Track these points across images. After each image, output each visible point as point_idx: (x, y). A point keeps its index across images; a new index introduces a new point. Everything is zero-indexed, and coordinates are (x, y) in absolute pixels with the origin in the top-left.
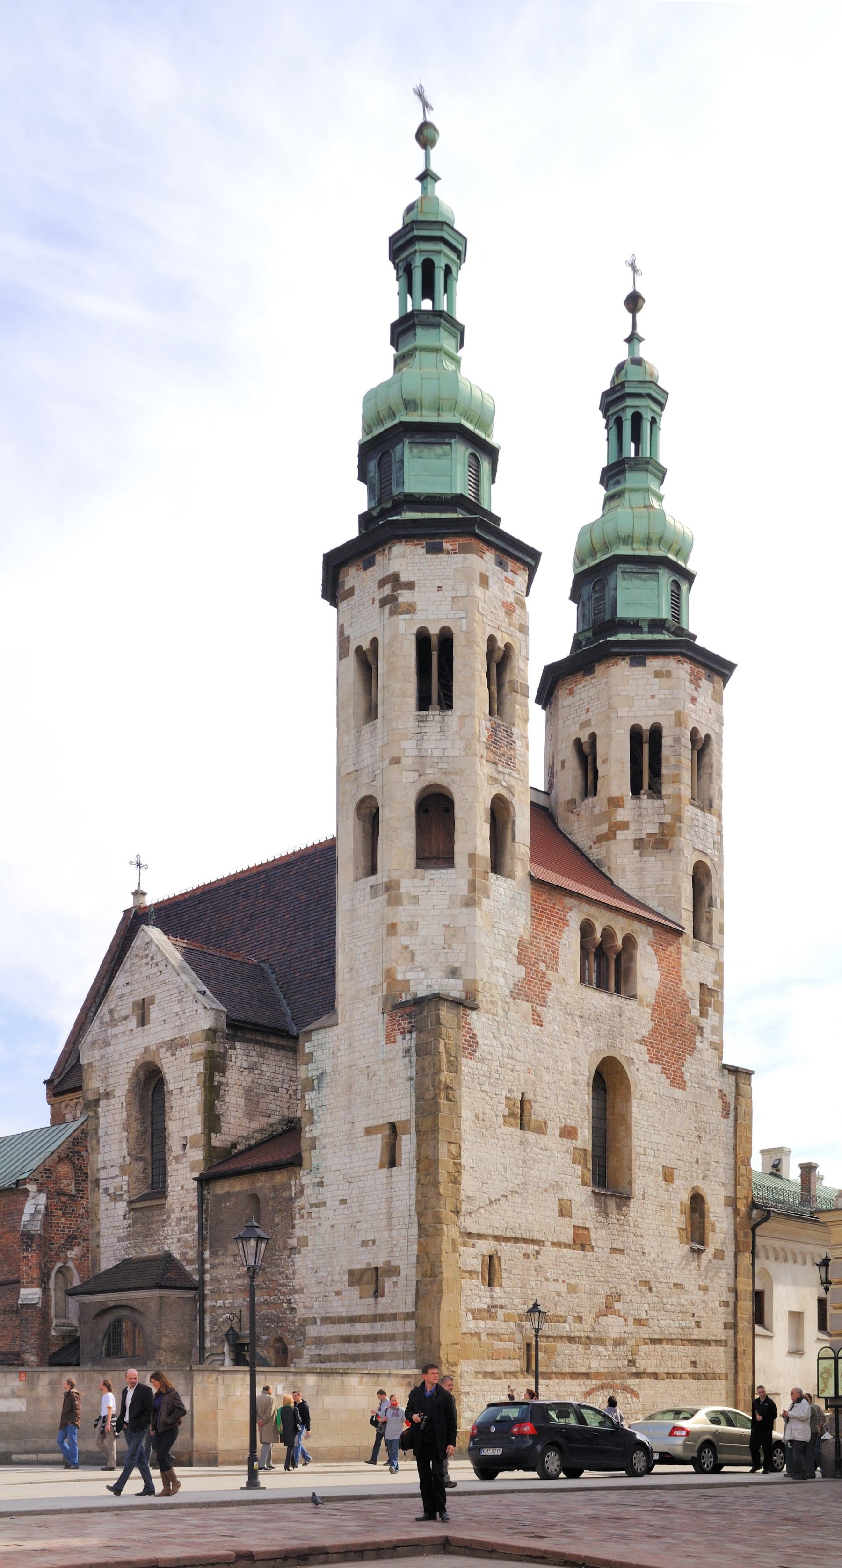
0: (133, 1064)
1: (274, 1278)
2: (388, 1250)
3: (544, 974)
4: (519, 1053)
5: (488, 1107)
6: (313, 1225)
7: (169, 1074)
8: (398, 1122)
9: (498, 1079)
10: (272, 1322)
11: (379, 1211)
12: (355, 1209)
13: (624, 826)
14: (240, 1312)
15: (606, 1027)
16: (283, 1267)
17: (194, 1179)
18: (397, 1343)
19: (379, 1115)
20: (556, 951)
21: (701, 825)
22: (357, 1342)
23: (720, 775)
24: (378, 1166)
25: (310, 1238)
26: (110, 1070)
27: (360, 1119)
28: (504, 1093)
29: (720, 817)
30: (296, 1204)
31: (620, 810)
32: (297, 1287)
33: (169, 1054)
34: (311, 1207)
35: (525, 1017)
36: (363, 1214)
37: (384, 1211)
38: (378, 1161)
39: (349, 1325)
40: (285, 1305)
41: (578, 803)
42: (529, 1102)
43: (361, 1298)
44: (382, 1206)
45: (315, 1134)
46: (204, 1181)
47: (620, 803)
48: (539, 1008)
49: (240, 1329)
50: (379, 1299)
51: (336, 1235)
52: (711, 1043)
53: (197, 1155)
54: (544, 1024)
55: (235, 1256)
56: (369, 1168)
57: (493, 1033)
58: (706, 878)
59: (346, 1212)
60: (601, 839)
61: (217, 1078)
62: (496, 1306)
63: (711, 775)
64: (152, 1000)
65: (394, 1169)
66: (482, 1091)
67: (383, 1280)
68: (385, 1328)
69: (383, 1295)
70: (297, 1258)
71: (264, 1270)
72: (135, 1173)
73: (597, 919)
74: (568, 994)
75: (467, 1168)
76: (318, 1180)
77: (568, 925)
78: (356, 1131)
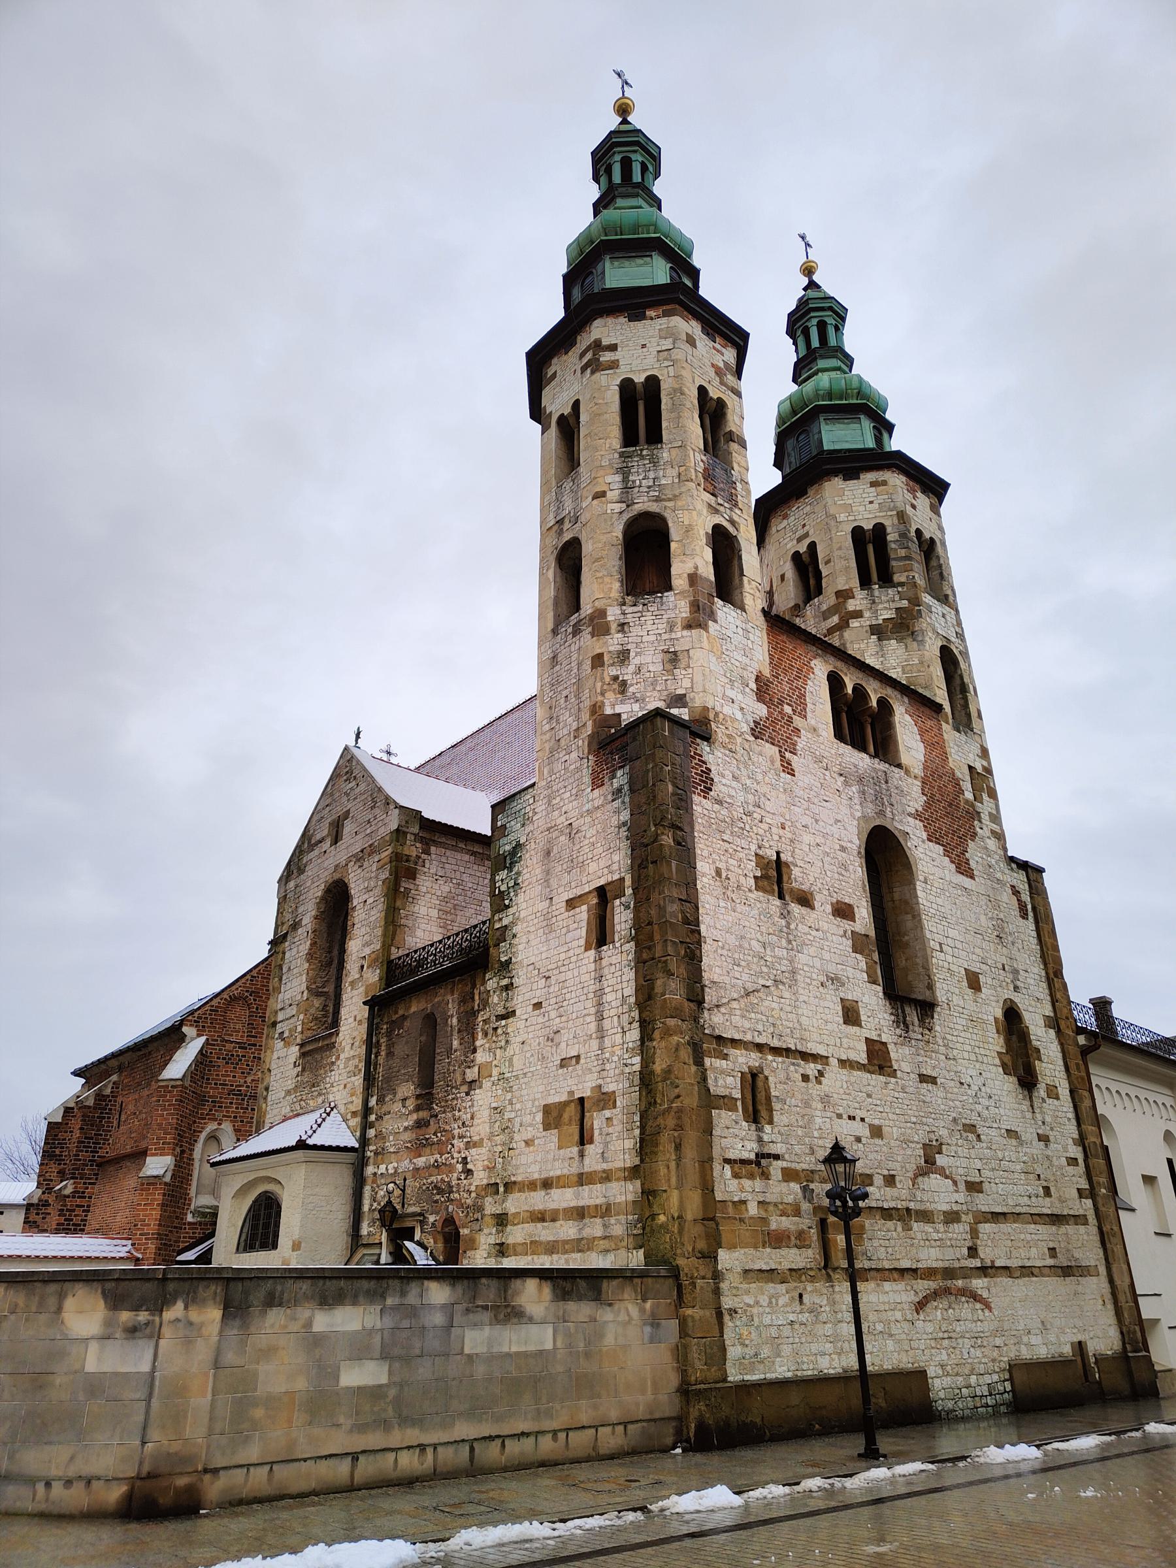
0: (323, 886)
1: (447, 1128)
2: (599, 1068)
3: (792, 718)
4: (768, 802)
5: (731, 861)
6: (499, 1045)
7: (355, 889)
8: (609, 884)
9: (743, 829)
10: (440, 1191)
11: (585, 1012)
12: (553, 1014)
13: (858, 614)
14: (405, 1180)
15: (872, 792)
16: (459, 1111)
17: (365, 1003)
18: (613, 1221)
19: (584, 880)
20: (802, 696)
21: (941, 614)
22: (553, 1220)
23: (950, 574)
24: (583, 948)
25: (494, 1063)
26: (301, 898)
27: (560, 890)
28: (754, 847)
29: (957, 611)
30: (480, 1019)
31: (850, 601)
32: (475, 1138)
33: (356, 867)
34: (497, 1021)
35: (772, 762)
36: (563, 1019)
37: (593, 1011)
38: (582, 942)
39: (543, 1193)
40: (460, 1167)
41: (802, 606)
42: (787, 865)
43: (560, 1148)
44: (589, 1004)
45: (505, 922)
46: (377, 1005)
47: (850, 595)
48: (788, 755)
49: (403, 1206)
50: (587, 1146)
51: (528, 1055)
52: (993, 832)
53: (373, 976)
54: (796, 774)
55: (404, 1100)
56: (571, 953)
57: (731, 772)
58: (952, 667)
59: (540, 1019)
60: (831, 631)
61: (404, 884)
62: (769, 1156)
63: (941, 574)
64: (347, 815)
65: (605, 948)
66: (724, 841)
67: (592, 1117)
68: (591, 1196)
69: (591, 1142)
70: (478, 1094)
71: (437, 1116)
72: (312, 1011)
73: (846, 675)
74: (822, 747)
75: (708, 941)
76: (505, 982)
77: (813, 673)
78: (554, 908)
